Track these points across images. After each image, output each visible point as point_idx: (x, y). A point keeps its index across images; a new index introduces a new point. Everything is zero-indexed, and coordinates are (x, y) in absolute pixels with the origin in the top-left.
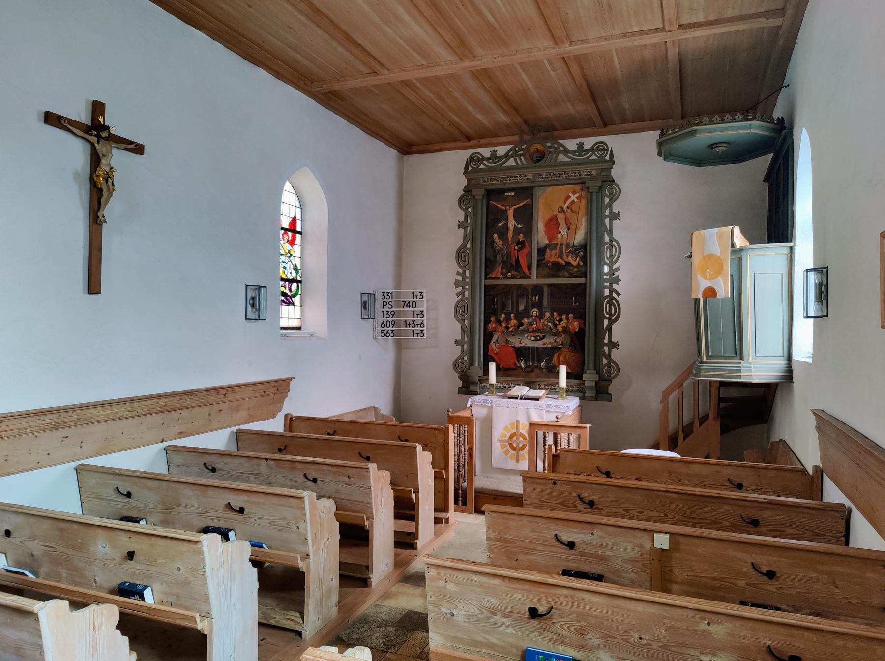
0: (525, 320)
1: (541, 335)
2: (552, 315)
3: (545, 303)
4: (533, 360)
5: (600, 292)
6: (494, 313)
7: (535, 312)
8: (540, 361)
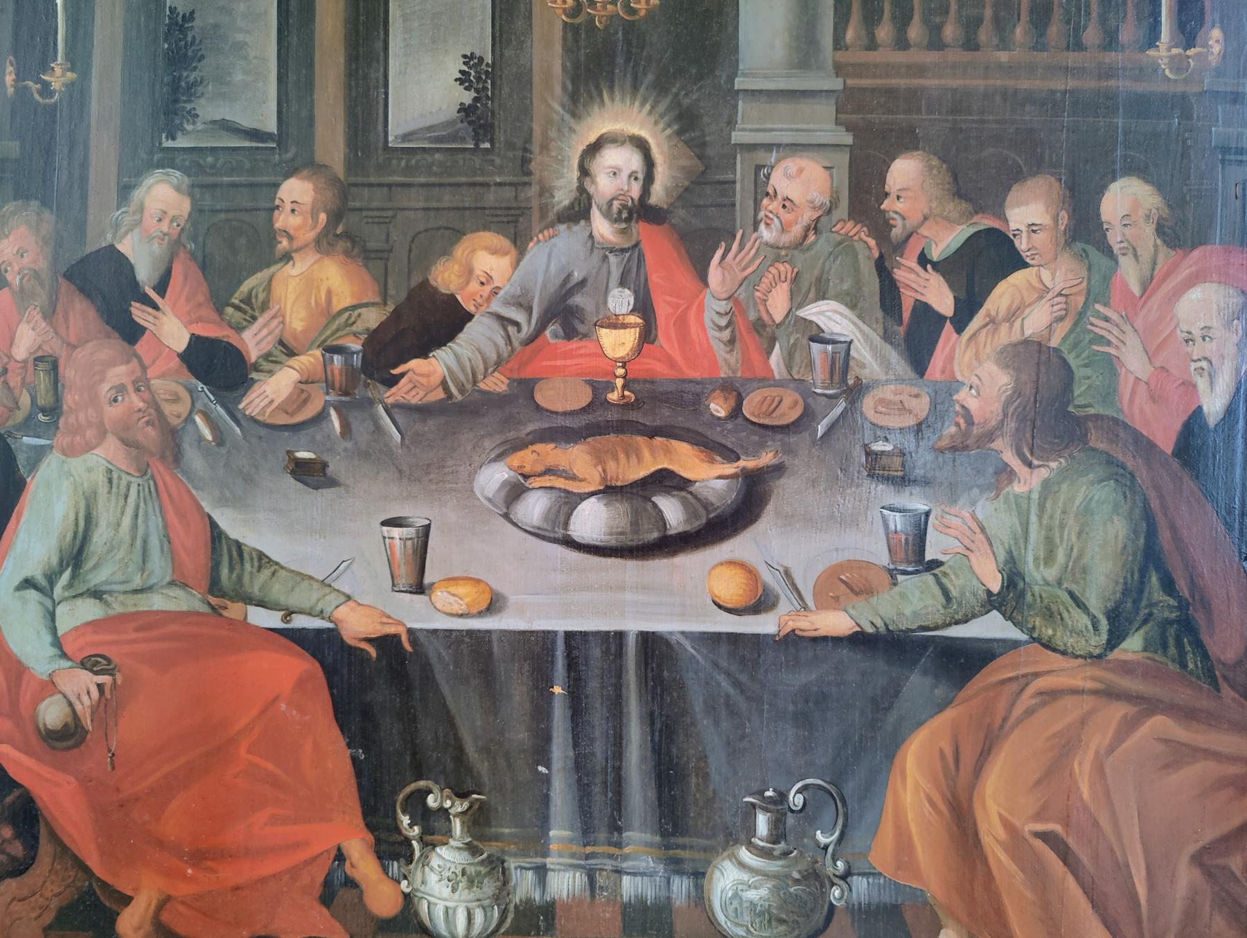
0: (481, 268)
1: (713, 479)
2: (864, 193)
4: (601, 816)
7: (618, 146)
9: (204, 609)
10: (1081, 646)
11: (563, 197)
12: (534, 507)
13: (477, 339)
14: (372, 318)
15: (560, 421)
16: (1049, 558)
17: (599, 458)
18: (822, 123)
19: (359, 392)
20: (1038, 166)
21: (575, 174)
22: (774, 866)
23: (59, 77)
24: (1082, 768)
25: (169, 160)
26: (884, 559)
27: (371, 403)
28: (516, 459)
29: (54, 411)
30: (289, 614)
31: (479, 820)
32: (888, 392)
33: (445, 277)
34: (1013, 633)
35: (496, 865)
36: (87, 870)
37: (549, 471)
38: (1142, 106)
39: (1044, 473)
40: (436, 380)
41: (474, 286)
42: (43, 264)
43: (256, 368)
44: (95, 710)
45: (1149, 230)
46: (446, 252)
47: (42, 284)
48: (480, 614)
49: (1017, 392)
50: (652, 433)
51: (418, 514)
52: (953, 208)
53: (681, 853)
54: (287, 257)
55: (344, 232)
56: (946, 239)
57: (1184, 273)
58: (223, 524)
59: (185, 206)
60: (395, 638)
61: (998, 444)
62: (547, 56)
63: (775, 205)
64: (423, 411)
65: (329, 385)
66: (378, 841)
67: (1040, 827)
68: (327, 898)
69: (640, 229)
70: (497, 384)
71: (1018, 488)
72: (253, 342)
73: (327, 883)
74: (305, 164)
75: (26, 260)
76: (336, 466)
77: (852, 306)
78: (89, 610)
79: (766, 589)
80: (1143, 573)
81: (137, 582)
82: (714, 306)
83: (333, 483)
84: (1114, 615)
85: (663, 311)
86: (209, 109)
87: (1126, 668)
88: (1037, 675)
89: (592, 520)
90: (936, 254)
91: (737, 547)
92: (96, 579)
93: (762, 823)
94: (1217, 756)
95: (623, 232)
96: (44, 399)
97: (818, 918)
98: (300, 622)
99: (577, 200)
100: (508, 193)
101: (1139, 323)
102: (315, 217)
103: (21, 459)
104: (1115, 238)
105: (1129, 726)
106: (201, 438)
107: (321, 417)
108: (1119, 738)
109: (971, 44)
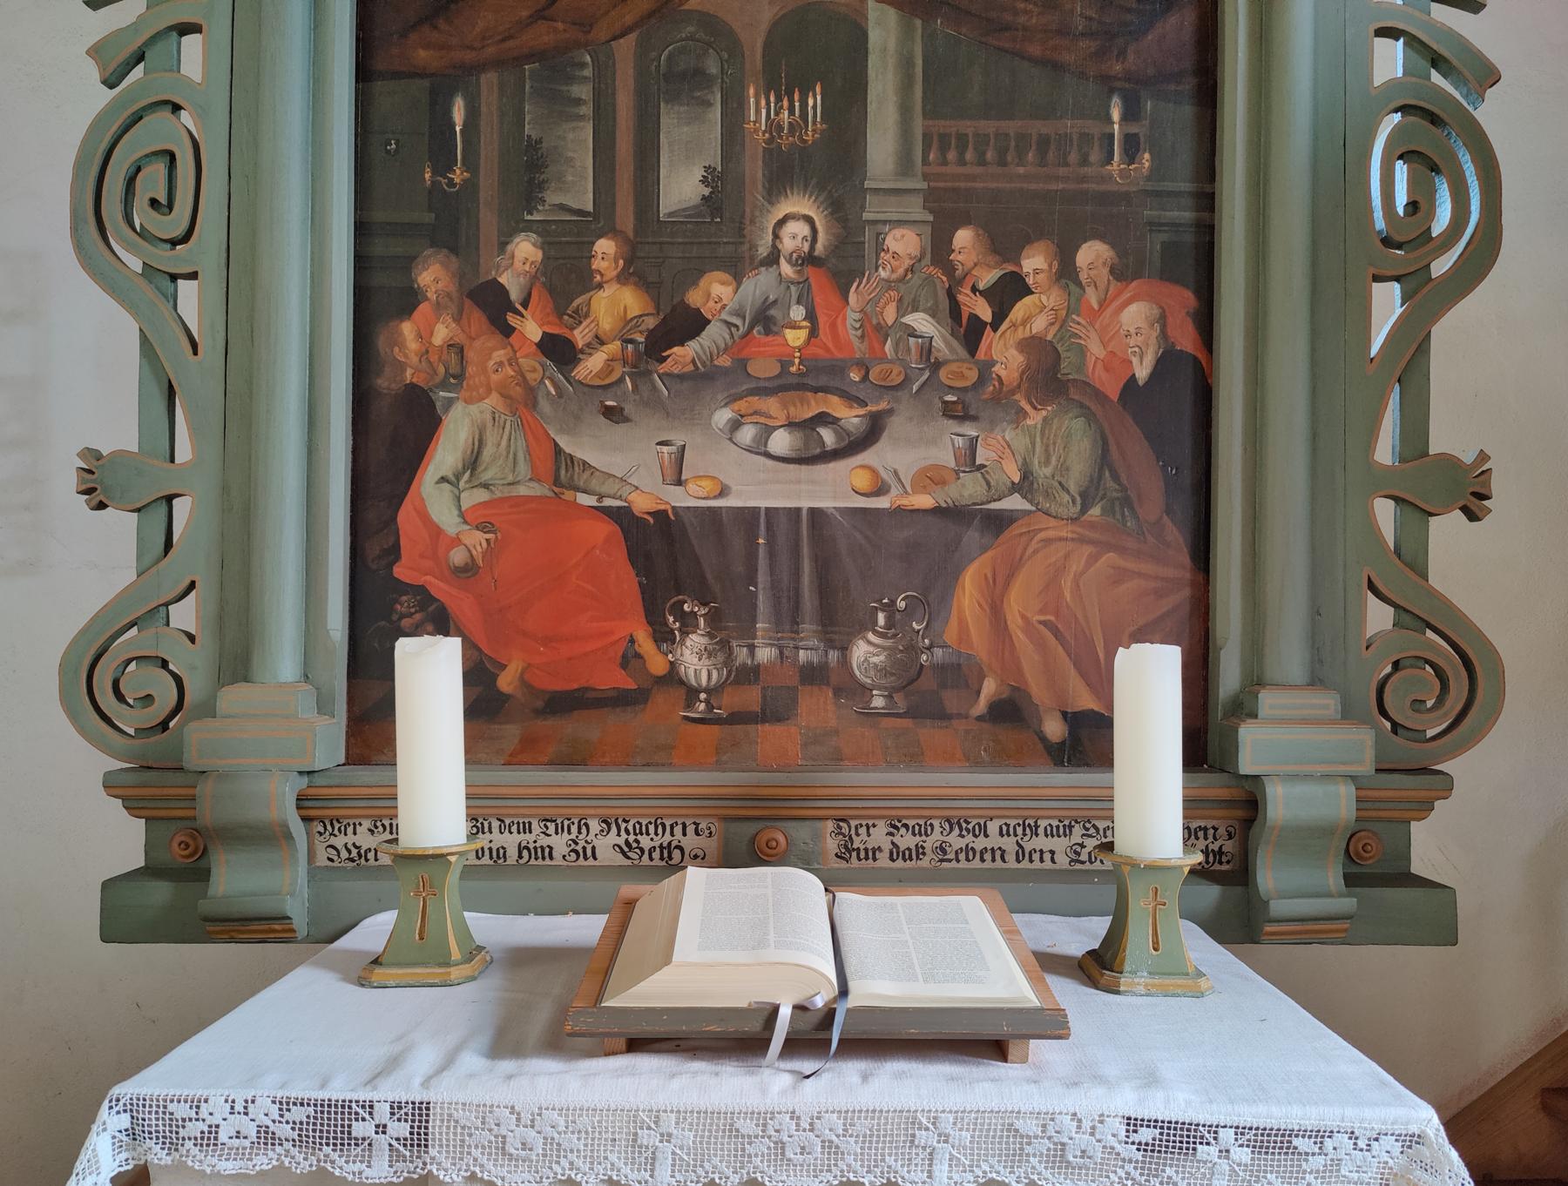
0: (715, 292)
1: (852, 418)
2: (940, 250)
3: (881, 148)
4: (788, 617)
5: (1342, 64)
6: (450, 227)
7: (796, 221)
8: (838, 625)
9: (550, 494)
10: (1063, 512)
11: (763, 251)
12: (747, 434)
13: (714, 334)
14: (651, 323)
15: (762, 384)
16: (1047, 462)
17: (785, 406)
18: (916, 209)
19: (642, 367)
20: (1041, 235)
21: (770, 237)
22: (888, 643)
23: (458, 175)
24: (1067, 584)
25: (529, 227)
26: (952, 464)
27: (650, 373)
28: (736, 406)
29: (460, 377)
30: (601, 498)
31: (714, 619)
32: (954, 367)
33: (694, 298)
34: (1028, 506)
35: (725, 645)
36: (479, 650)
37: (755, 413)
38: (1105, 198)
39: (1044, 413)
40: (689, 359)
41: (711, 304)
42: (453, 289)
43: (582, 352)
44: (484, 554)
45: (1105, 271)
46: (695, 283)
47: (451, 299)
48: (715, 497)
49: (1028, 367)
50: (816, 390)
51: (678, 438)
52: (991, 259)
53: (836, 637)
54: (600, 286)
55: (633, 271)
56: (987, 278)
57: (1127, 295)
58: (562, 444)
59: (539, 255)
60: (665, 511)
61: (1017, 397)
62: (754, 169)
63: (888, 257)
64: (681, 377)
65: (625, 363)
66: (655, 631)
67: (1042, 618)
68: (625, 663)
69: (809, 271)
70: (725, 361)
71: (1029, 422)
72: (580, 336)
73: (624, 656)
74: (610, 231)
75: (440, 285)
76: (629, 409)
77: (933, 316)
78: (482, 496)
79: (883, 481)
80: (1101, 470)
81: (510, 478)
82: (852, 316)
83: (627, 420)
84: (1084, 495)
85: (822, 320)
86: (553, 197)
87: (1092, 526)
88: (1041, 530)
89: (781, 441)
90: (981, 286)
91: (867, 457)
92: (486, 477)
93: (881, 618)
94: (1140, 575)
95: (799, 272)
96: (454, 369)
97: (913, 672)
98: (608, 502)
99: (771, 253)
100: (730, 248)
101: (1097, 326)
102: (616, 262)
103: (438, 405)
104: (1083, 277)
105: (1093, 559)
106: (549, 393)
107: (621, 380)
108: (1089, 565)
109: (1002, 162)
